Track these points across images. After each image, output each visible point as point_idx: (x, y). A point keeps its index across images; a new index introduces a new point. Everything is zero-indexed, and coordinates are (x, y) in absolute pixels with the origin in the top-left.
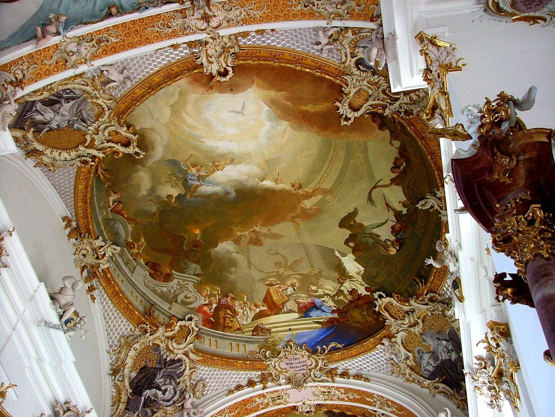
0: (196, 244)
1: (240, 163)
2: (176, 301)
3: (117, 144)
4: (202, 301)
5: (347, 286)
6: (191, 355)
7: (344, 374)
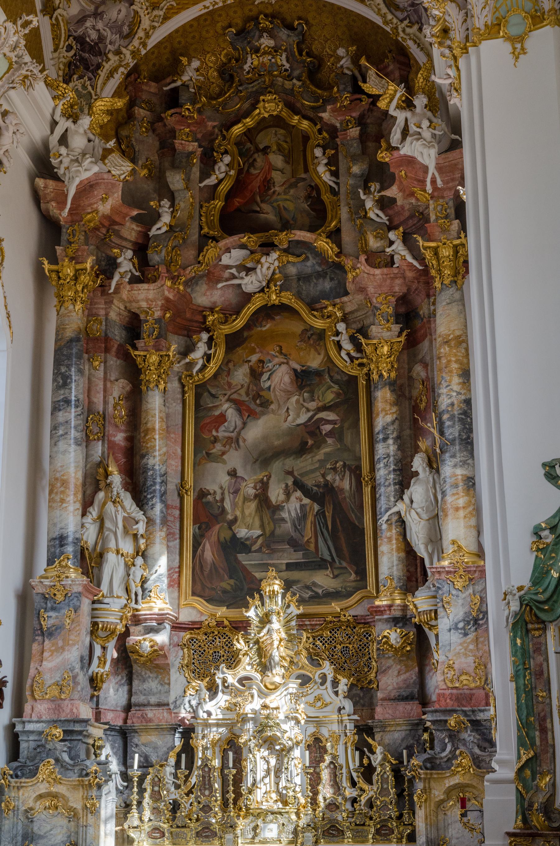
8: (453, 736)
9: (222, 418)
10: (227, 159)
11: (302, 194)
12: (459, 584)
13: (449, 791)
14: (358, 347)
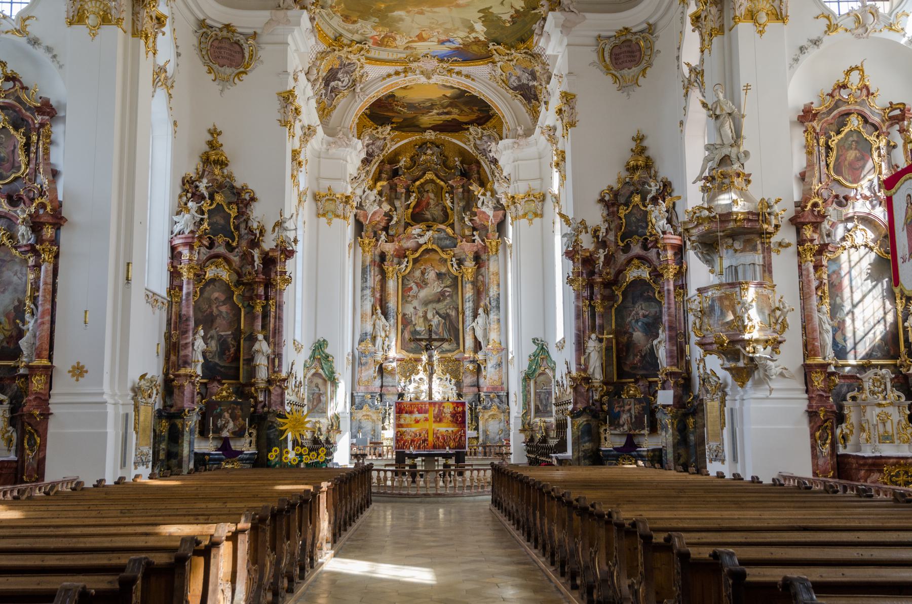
0: (380, 11)
2: (357, 33)
4: (375, 33)
5: (474, 35)
6: (362, 60)
7: (459, 73)
8: (491, 400)
9: (411, 289)
10: (414, 195)
11: (440, 209)
14: (460, 267)
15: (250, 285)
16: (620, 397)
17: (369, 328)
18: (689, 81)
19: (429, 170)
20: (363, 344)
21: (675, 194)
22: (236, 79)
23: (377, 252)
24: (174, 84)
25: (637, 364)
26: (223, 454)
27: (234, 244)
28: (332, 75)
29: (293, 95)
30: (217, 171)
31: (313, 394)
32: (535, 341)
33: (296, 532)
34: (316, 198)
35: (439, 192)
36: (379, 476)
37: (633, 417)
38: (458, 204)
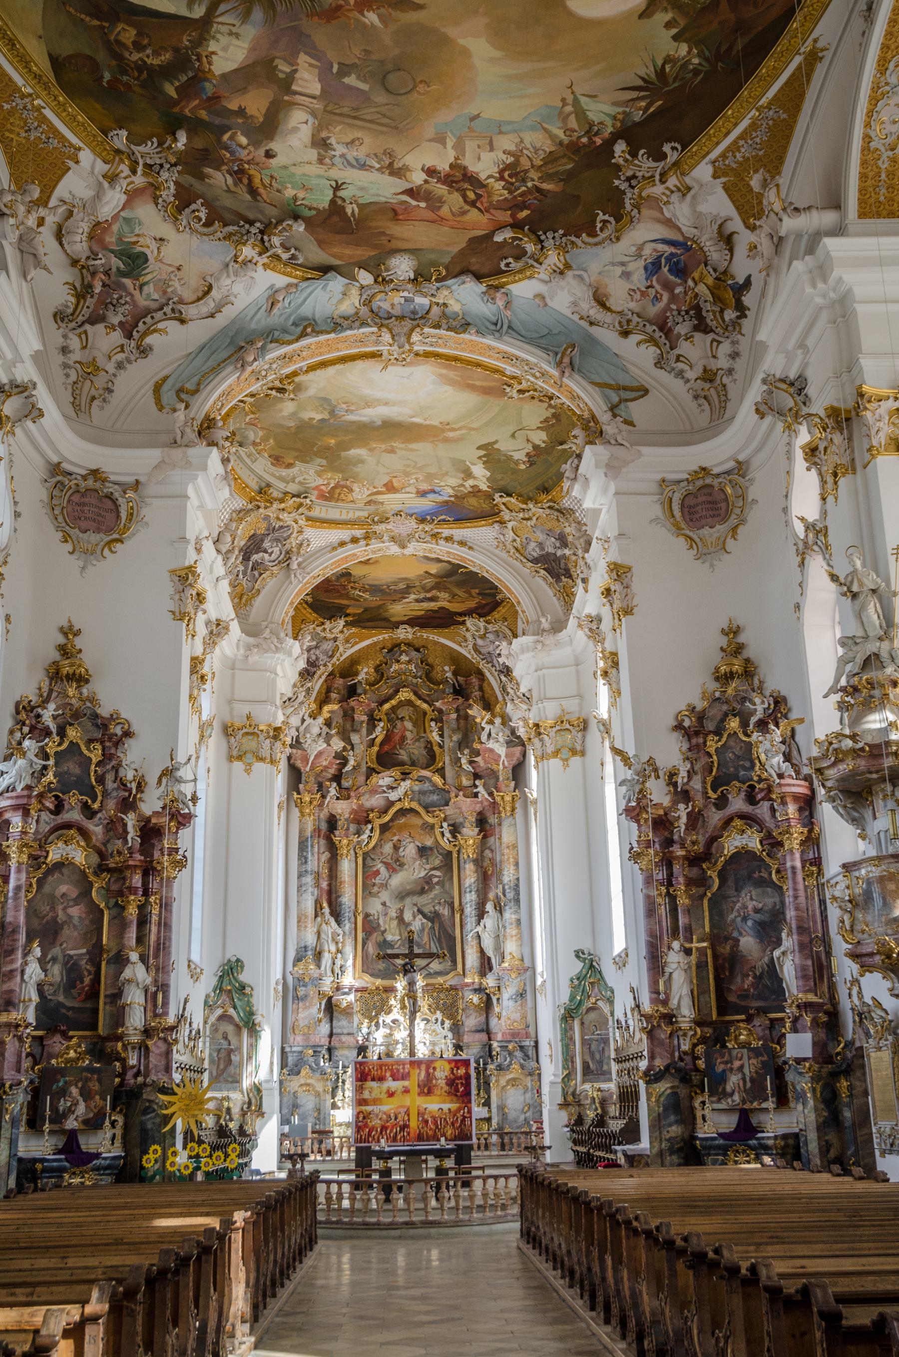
0: (328, 448)
1: (394, 404)
3: (271, 389)
4: (321, 482)
5: (471, 482)
6: (300, 522)
7: (448, 539)
8: (511, 1054)
9: (378, 872)
10: (382, 724)
11: (423, 745)
12: (513, 976)
13: (508, 1082)
14: (454, 837)
15: (119, 872)
16: (724, 1046)
17: (310, 939)
18: (806, 543)
19: (404, 686)
20: (301, 965)
21: (793, 715)
22: (106, 552)
23: (324, 814)
24: (8, 560)
25: (748, 990)
26: (67, 1160)
27: (96, 806)
28: (254, 545)
29: (194, 573)
30: (71, 692)
31: (219, 1051)
32: (578, 954)
33: (189, 1308)
34: (228, 731)
35: (420, 720)
36: (328, 1193)
37: (748, 1079)
38: (451, 737)
